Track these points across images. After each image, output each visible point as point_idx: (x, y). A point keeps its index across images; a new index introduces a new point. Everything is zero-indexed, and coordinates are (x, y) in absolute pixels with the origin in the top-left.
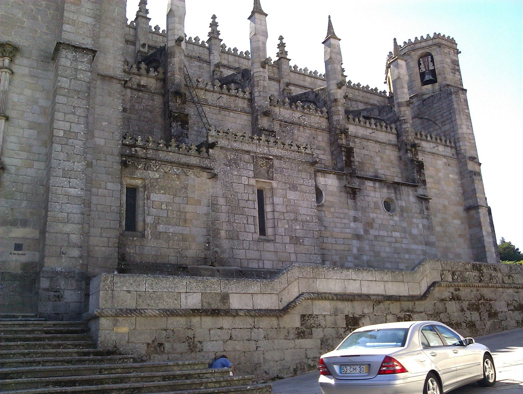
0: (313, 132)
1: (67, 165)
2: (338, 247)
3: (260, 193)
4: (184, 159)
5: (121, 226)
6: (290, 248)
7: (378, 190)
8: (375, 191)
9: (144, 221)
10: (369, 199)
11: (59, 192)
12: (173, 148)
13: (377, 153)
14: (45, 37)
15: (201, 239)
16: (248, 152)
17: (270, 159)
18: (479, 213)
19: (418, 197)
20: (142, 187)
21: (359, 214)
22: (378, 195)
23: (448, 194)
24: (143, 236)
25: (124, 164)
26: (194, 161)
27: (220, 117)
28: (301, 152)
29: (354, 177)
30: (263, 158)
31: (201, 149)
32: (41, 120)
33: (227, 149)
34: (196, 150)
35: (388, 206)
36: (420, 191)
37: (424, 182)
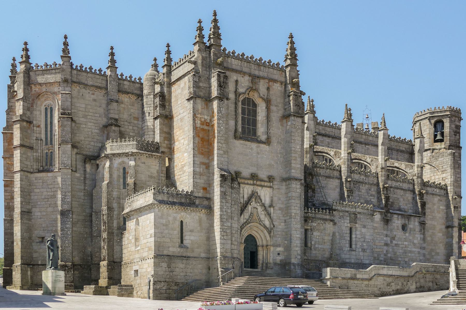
0: (370, 186)
1: (296, 226)
2: (377, 250)
3: (351, 229)
4: (325, 217)
7: (400, 219)
8: (398, 220)
9: (311, 243)
10: (395, 224)
11: (294, 236)
13: (401, 196)
14: (281, 171)
16: (348, 212)
17: (356, 214)
19: (420, 222)
20: (310, 229)
21: (389, 233)
22: (399, 222)
23: (438, 218)
24: (311, 249)
25: (306, 221)
26: (328, 217)
27: (325, 182)
28: (369, 210)
29: (388, 213)
30: (353, 214)
31: (330, 212)
32: (282, 206)
33: (340, 211)
35: (404, 228)
36: (422, 219)
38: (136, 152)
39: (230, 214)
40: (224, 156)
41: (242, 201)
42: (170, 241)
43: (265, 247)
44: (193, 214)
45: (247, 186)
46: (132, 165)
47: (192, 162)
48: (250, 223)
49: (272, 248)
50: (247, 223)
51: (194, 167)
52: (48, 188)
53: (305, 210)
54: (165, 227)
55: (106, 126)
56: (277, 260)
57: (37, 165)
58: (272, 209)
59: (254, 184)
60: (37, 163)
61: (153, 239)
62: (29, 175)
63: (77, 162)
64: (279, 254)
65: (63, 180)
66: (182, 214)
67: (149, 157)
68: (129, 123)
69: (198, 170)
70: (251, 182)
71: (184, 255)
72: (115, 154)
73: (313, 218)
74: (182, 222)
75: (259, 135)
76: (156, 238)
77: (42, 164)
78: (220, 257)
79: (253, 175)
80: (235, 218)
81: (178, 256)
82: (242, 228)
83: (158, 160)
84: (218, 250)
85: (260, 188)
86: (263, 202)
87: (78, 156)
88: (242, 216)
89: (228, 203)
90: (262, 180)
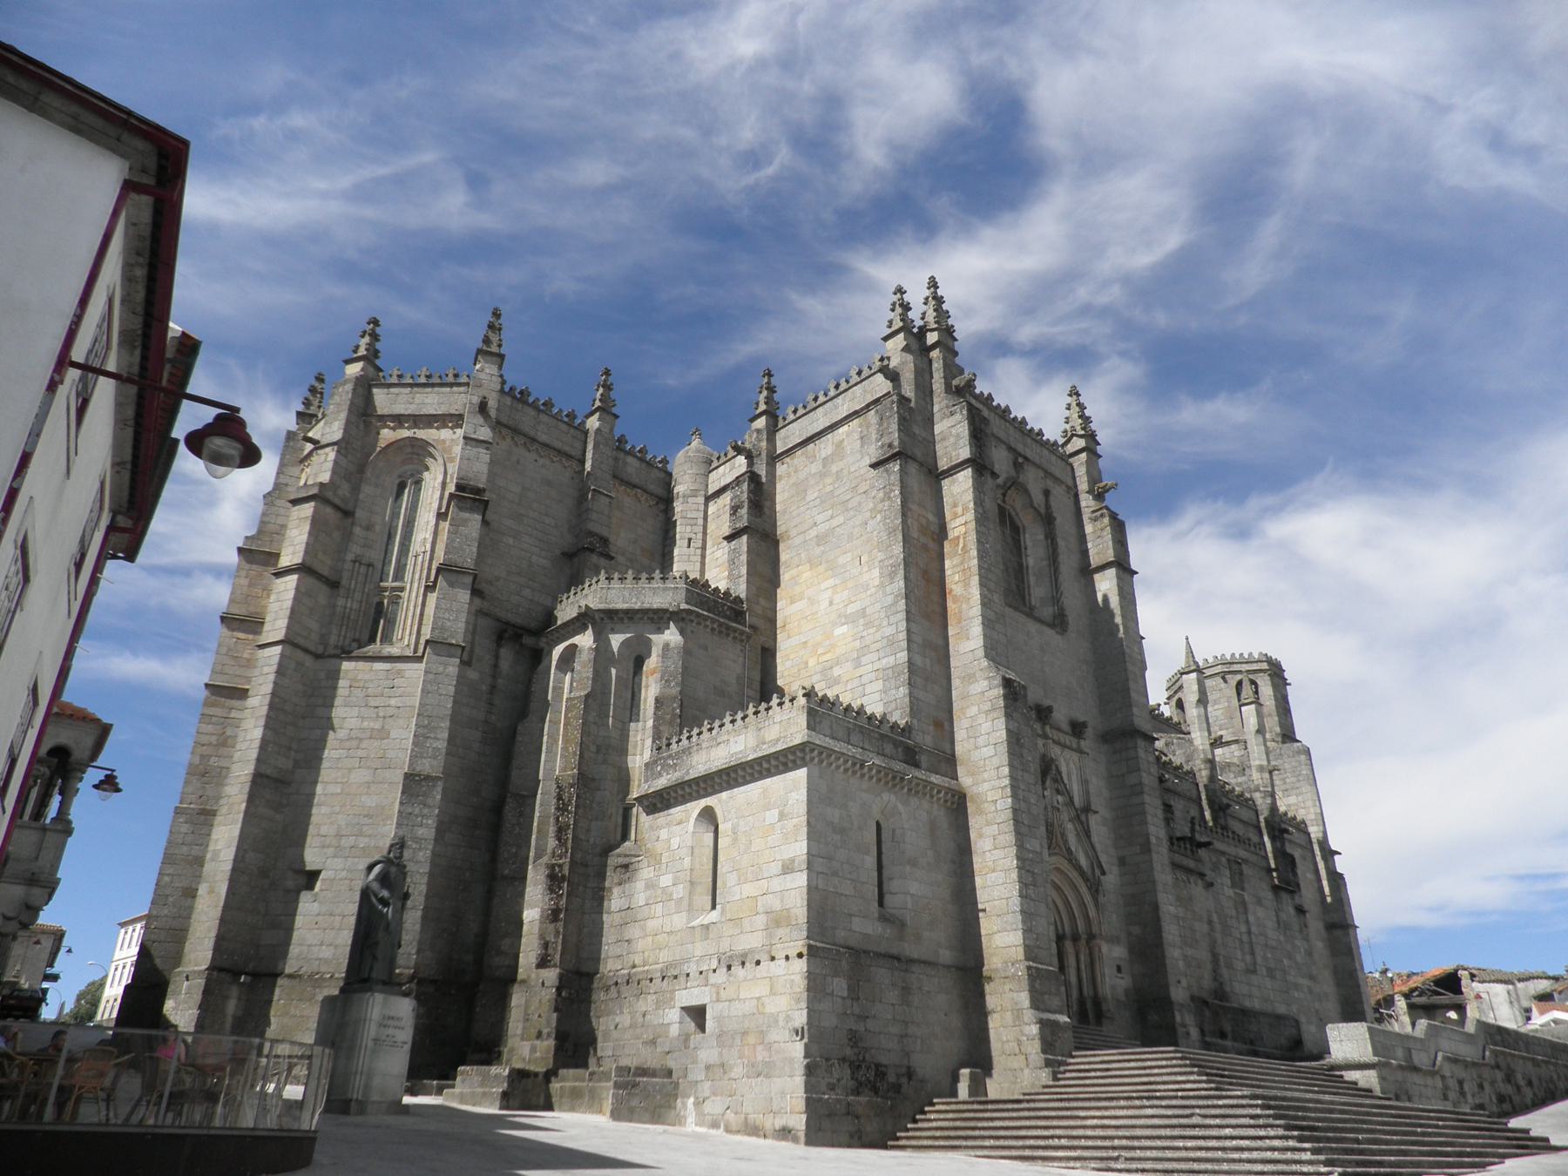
6: (1268, 983)
15: (1209, 967)
16: (1223, 853)
18: (1348, 934)
26: (1191, 864)
28: (1257, 854)
34: (1191, 850)
37: (1298, 885)
38: (688, 612)
44: (914, 801)
46: (672, 645)
47: (903, 636)
51: (909, 649)
54: (837, 837)
55: (569, 556)
57: (343, 633)
60: (344, 627)
61: (801, 879)
62: (308, 661)
63: (477, 638)
64: (1119, 969)
65: (431, 676)
66: (886, 796)
67: (720, 632)
69: (918, 660)
71: (894, 951)
77: (357, 634)
78: (1027, 963)
81: (879, 955)
87: (483, 622)
89: (1027, 771)
90: (1059, 729)
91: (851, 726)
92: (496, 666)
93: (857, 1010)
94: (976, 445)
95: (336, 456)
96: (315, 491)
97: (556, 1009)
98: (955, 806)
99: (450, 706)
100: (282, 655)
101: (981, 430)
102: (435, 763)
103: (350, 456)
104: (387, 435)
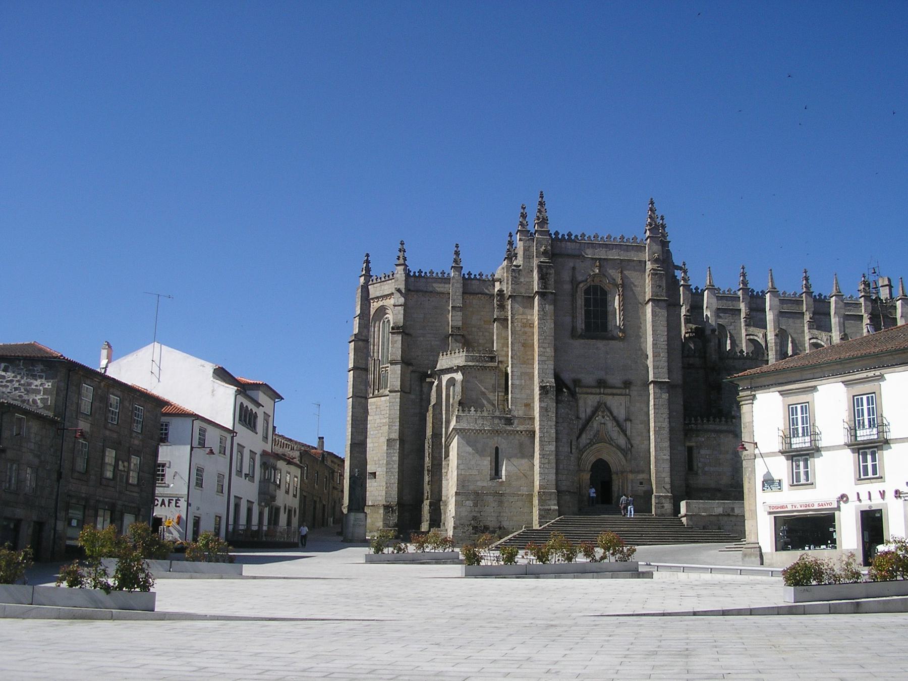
5: (686, 469)
12: (711, 422)
24: (697, 474)
25: (686, 435)
26: (725, 428)
34: (725, 421)
39: (554, 435)
40: (547, 362)
41: (583, 415)
42: (477, 473)
43: (620, 475)
45: (591, 397)
48: (594, 444)
49: (630, 476)
50: (591, 443)
52: (381, 414)
53: (685, 420)
56: (639, 491)
58: (629, 424)
59: (600, 394)
64: (641, 483)
66: (496, 438)
68: (478, 328)
70: (598, 391)
72: (443, 370)
73: (698, 431)
74: (497, 449)
75: (610, 329)
76: (459, 470)
79: (599, 381)
80: (564, 440)
82: (581, 451)
83: (493, 372)
84: (537, 483)
85: (611, 397)
86: (615, 414)
88: (584, 436)
89: (550, 421)
91: (477, 417)
92: (421, 391)
93: (477, 510)
94: (542, 283)
95: (359, 321)
96: (353, 338)
97: (430, 513)
98: (533, 435)
99: (398, 413)
100: (353, 402)
101: (547, 274)
102: (396, 434)
103: (365, 319)
104: (375, 306)
